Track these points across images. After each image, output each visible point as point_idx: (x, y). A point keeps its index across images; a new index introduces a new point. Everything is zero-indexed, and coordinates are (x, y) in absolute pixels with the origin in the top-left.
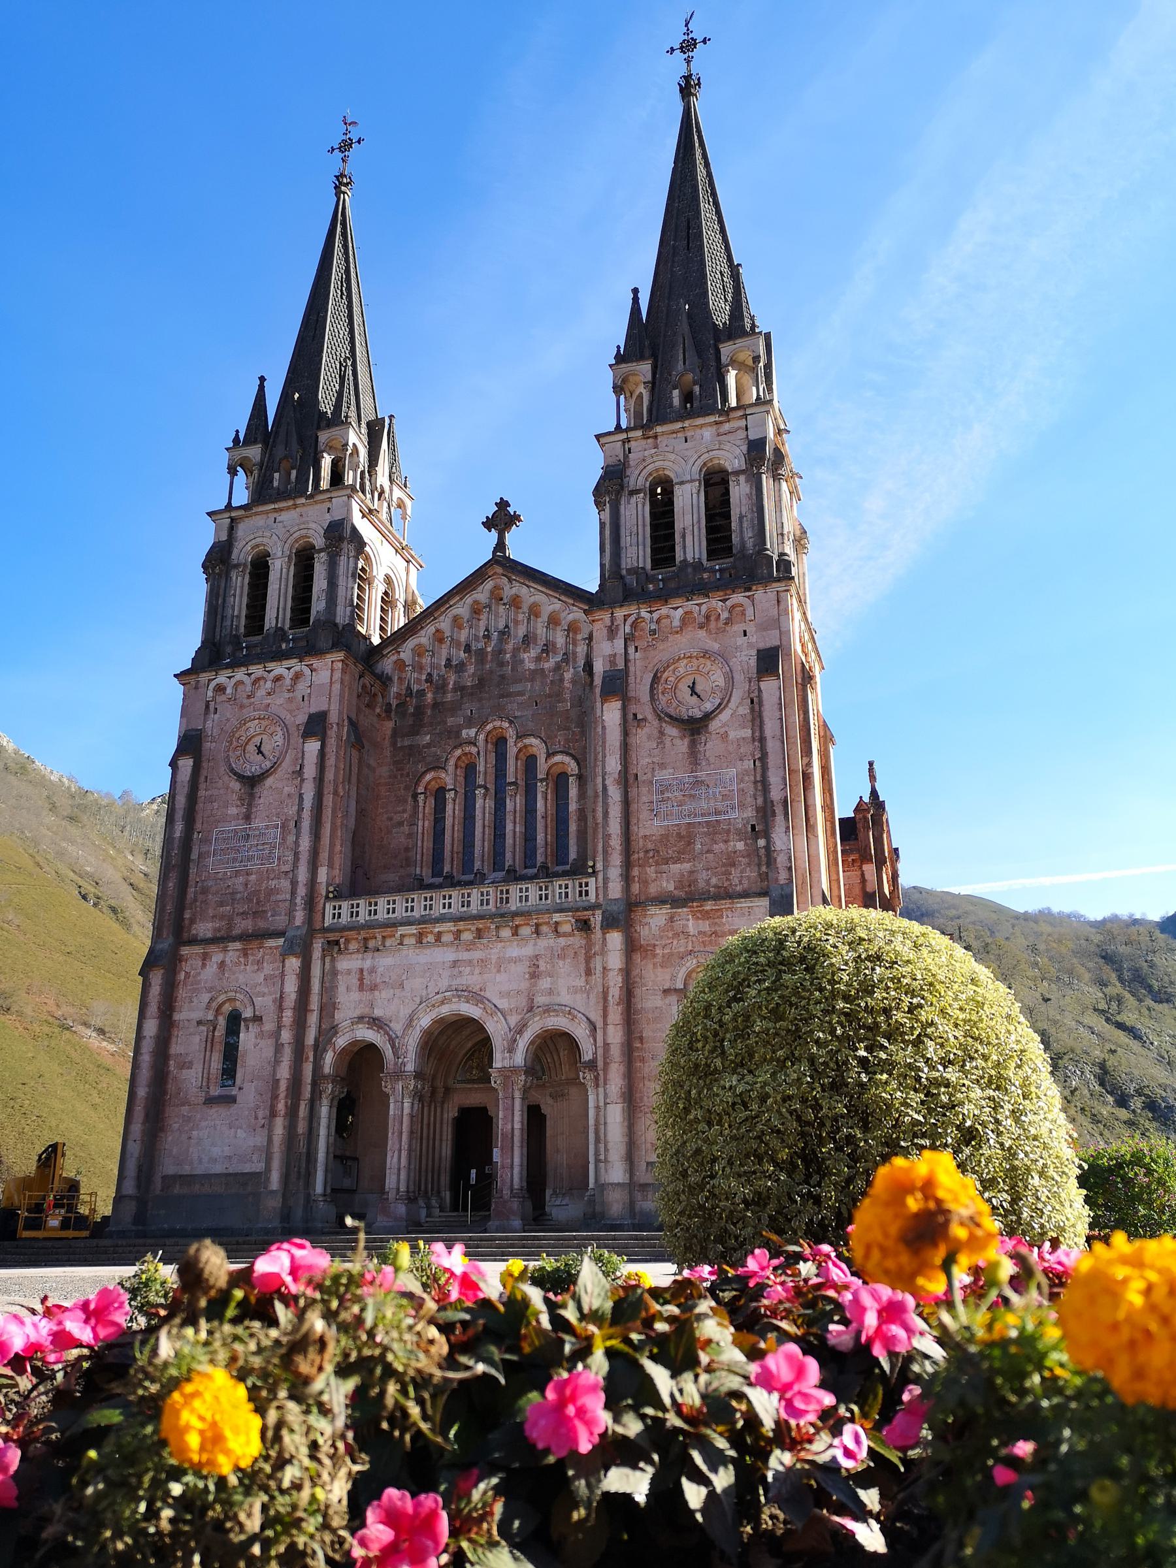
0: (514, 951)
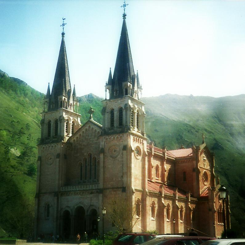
0: (88, 196)
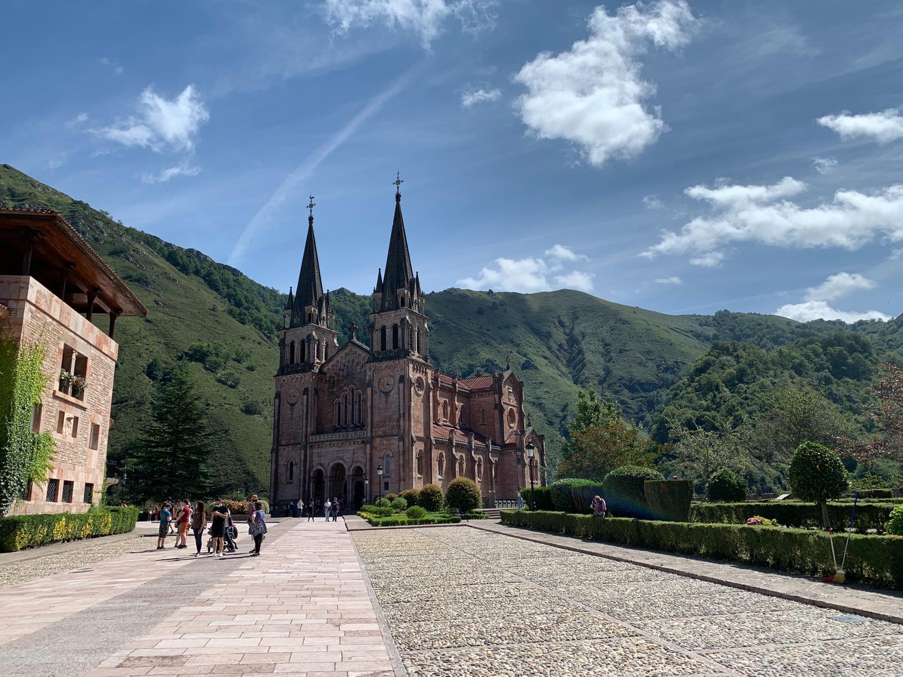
0: (350, 448)
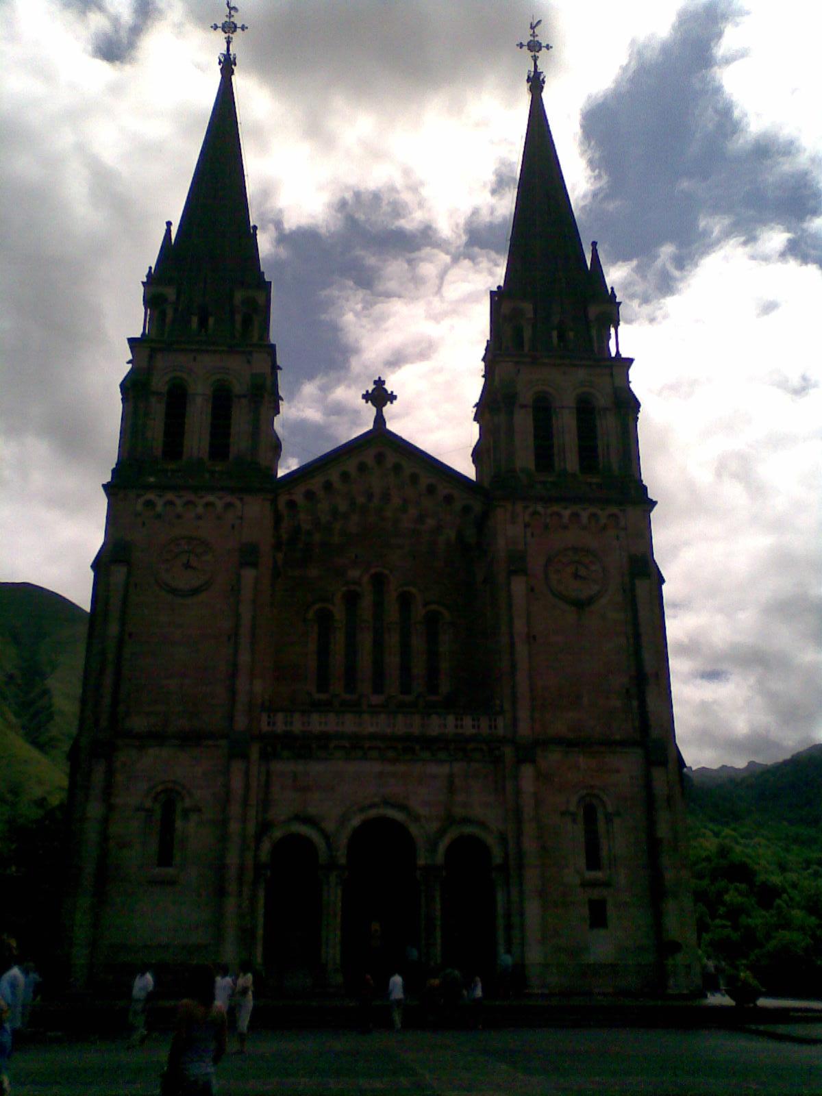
0: (434, 769)
